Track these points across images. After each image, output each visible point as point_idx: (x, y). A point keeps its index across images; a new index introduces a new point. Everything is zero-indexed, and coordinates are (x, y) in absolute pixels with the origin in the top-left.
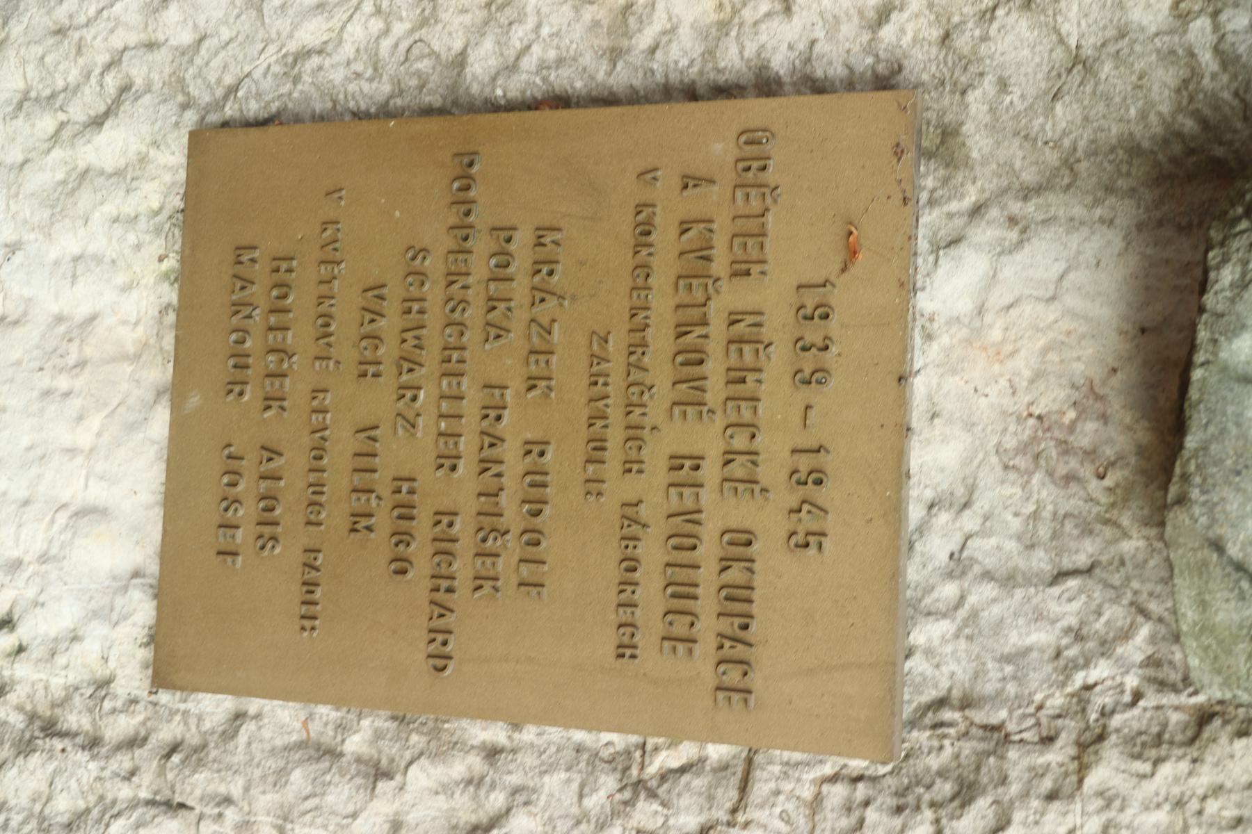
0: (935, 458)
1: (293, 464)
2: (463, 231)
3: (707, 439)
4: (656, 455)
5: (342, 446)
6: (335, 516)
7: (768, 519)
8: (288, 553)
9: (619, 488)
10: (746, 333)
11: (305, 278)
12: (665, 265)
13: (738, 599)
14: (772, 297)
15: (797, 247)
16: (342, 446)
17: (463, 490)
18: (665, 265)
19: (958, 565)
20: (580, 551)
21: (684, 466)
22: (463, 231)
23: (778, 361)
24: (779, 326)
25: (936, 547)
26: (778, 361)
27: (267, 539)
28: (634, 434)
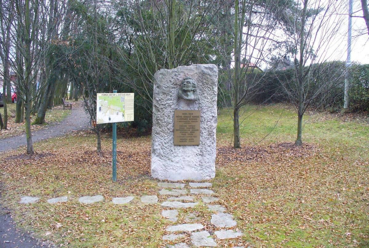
0: (189, 109)
1: (190, 138)
2: (180, 130)
3: (188, 118)
4: (189, 120)
5: (189, 136)
6: (192, 136)
7: (192, 116)
8: (193, 138)
9: (191, 122)
10: (184, 117)
11: (181, 138)
12: (181, 120)
13: (195, 117)
14: (183, 116)
15: (181, 115)
16: (189, 136)
17: (191, 129)
18: (181, 120)
19: (193, 108)
20: (193, 124)
21: (190, 119)
22: (180, 130)
23: (185, 115)
24: (184, 115)
25: (192, 109)
26: (185, 115)
27: (193, 139)
28: (189, 121)
